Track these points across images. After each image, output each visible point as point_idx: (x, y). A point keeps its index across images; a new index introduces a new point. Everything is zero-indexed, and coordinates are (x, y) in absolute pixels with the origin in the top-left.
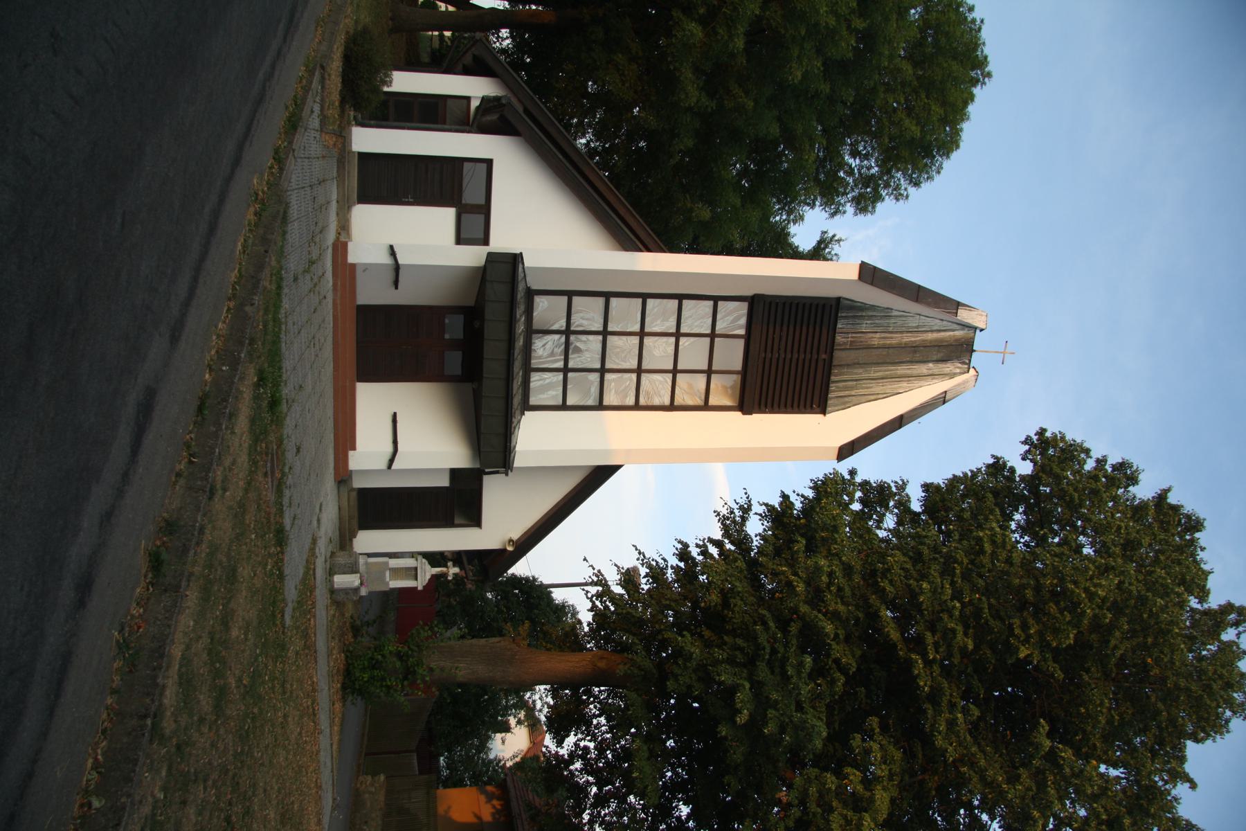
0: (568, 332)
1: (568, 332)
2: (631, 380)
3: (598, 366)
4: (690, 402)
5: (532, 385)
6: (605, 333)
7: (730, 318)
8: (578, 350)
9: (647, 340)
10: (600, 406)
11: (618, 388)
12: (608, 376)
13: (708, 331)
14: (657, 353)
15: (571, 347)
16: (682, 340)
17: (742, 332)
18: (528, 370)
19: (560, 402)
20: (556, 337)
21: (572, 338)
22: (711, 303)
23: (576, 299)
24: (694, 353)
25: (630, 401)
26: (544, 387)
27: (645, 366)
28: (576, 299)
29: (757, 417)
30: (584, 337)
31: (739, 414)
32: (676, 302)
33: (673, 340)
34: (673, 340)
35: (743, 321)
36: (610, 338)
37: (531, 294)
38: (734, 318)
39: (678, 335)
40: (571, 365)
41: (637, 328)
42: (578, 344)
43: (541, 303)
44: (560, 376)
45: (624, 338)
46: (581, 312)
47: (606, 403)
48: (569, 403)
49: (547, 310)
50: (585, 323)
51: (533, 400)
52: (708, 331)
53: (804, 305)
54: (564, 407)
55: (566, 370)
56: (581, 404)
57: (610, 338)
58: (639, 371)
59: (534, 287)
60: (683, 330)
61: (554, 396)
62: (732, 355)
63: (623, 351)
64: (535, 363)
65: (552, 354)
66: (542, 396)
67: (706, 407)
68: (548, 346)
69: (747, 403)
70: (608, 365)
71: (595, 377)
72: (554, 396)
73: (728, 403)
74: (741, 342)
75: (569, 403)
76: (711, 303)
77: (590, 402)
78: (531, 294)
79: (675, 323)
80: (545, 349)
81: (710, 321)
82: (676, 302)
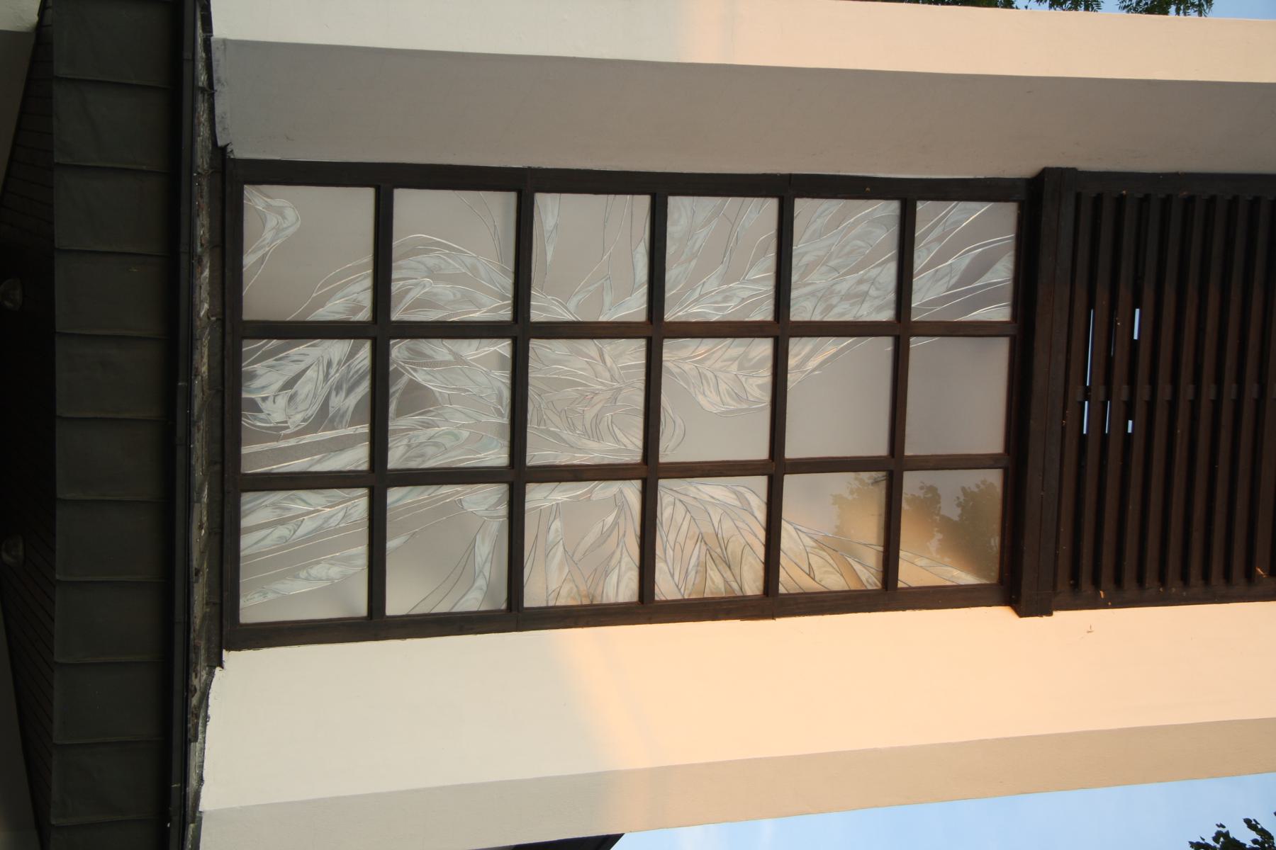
0: (380, 329)
1: (380, 329)
2: (621, 505)
3: (497, 456)
4: (834, 581)
5: (247, 543)
6: (520, 330)
7: (959, 262)
8: (419, 399)
9: (676, 354)
10: (514, 614)
11: (580, 538)
12: (538, 497)
13: (887, 315)
14: (709, 401)
15: (396, 389)
16: (799, 349)
17: (1000, 312)
18: (233, 484)
19: (360, 607)
20: (337, 349)
21: (399, 350)
22: (888, 210)
23: (407, 202)
24: (837, 398)
25: (623, 588)
26: (294, 549)
27: (669, 452)
28: (407, 202)
29: (1068, 624)
30: (441, 349)
31: (1002, 615)
32: (771, 205)
33: (763, 348)
34: (763, 348)
35: (1002, 273)
36: (540, 349)
37: (235, 176)
38: (970, 257)
39: (781, 329)
40: (396, 458)
41: (634, 307)
42: (420, 377)
43: (273, 216)
44: (357, 503)
45: (590, 347)
46: (427, 247)
47: (534, 597)
48: (395, 606)
49: (296, 246)
50: (444, 290)
51: (255, 606)
52: (887, 315)
53: (1212, 200)
54: (375, 624)
55: (378, 479)
56: (443, 608)
57: (540, 349)
58: (650, 471)
59: (242, 151)
60: (801, 311)
61: (335, 584)
62: (967, 401)
63: (587, 398)
64: (256, 456)
65: (323, 418)
66: (298, 587)
67: (888, 594)
68: (304, 388)
69: (1027, 576)
70: (537, 455)
71: (487, 501)
72: (335, 584)
73: (966, 578)
74: (998, 353)
75: (395, 606)
76: (888, 210)
77: (473, 601)
78: (235, 176)
79: (768, 288)
80: (293, 399)
81: (888, 274)
82: (771, 205)
